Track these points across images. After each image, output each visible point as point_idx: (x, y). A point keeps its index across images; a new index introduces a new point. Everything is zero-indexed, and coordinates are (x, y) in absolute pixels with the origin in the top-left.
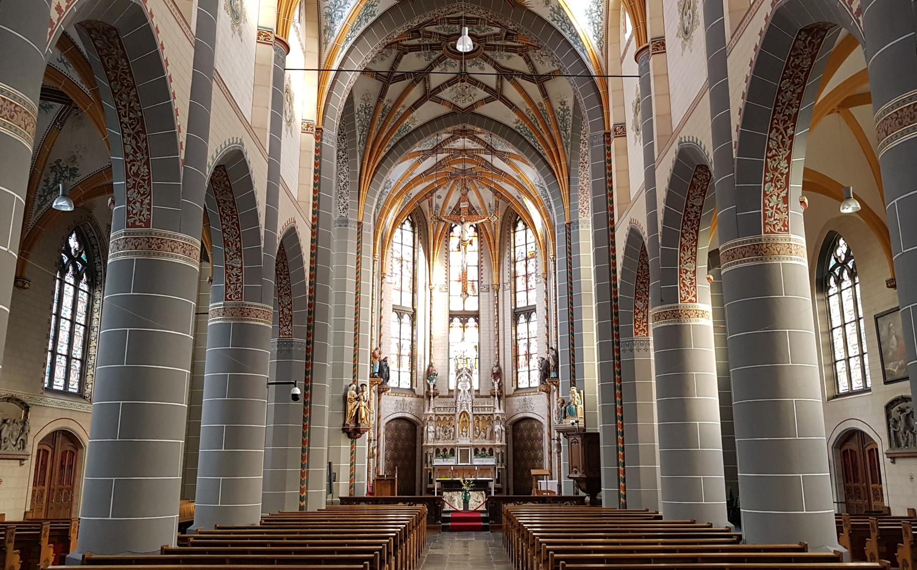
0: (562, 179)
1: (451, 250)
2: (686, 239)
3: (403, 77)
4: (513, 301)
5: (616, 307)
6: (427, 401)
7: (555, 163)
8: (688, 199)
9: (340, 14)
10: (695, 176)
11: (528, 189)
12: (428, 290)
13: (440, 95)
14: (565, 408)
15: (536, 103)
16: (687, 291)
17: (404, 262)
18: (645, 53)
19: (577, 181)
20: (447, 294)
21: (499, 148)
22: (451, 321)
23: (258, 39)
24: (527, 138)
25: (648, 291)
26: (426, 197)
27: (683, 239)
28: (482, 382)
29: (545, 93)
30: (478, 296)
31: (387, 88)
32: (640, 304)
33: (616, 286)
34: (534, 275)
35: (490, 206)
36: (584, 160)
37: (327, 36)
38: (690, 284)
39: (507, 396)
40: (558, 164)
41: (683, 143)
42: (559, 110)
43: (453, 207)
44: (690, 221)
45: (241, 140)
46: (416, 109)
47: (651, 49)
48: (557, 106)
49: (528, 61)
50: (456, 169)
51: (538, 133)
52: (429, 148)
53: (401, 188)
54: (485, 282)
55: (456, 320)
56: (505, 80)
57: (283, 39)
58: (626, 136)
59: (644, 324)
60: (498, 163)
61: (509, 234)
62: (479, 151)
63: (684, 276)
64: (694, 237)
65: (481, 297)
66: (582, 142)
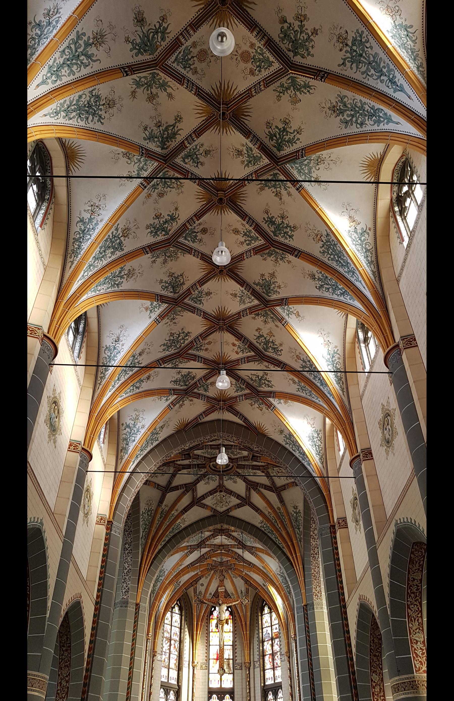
0: (298, 567)
1: (211, 631)
2: (412, 611)
3: (176, 488)
4: (262, 678)
5: (355, 681)
7: (292, 555)
8: (409, 573)
9: (133, 438)
10: (412, 553)
11: (271, 577)
12: (191, 668)
13: (204, 501)
15: (276, 507)
16: (420, 662)
17: (173, 642)
18: (357, 461)
19: (310, 569)
20: (207, 671)
21: (248, 544)
23: (69, 448)
24: (270, 535)
25: (381, 665)
26: (192, 585)
27: (409, 611)
29: (281, 500)
30: (233, 673)
31: (166, 495)
32: (375, 677)
33: (352, 659)
34: (278, 653)
35: (242, 592)
36: (314, 552)
37: (122, 454)
38: (422, 654)
40: (294, 555)
41: (399, 524)
42: (293, 513)
43: (213, 594)
44: (414, 593)
45: (41, 520)
46: (186, 512)
47: (361, 457)
48: (291, 510)
49: (268, 476)
50: (215, 561)
51: (277, 530)
52: (195, 543)
53: (172, 577)
55: (214, 696)
56: (252, 491)
57: (88, 449)
58: (347, 527)
59: (382, 698)
60: (248, 556)
61: (257, 616)
62: (233, 546)
63: (415, 646)
64: (418, 608)
65: (235, 675)
66: (312, 537)
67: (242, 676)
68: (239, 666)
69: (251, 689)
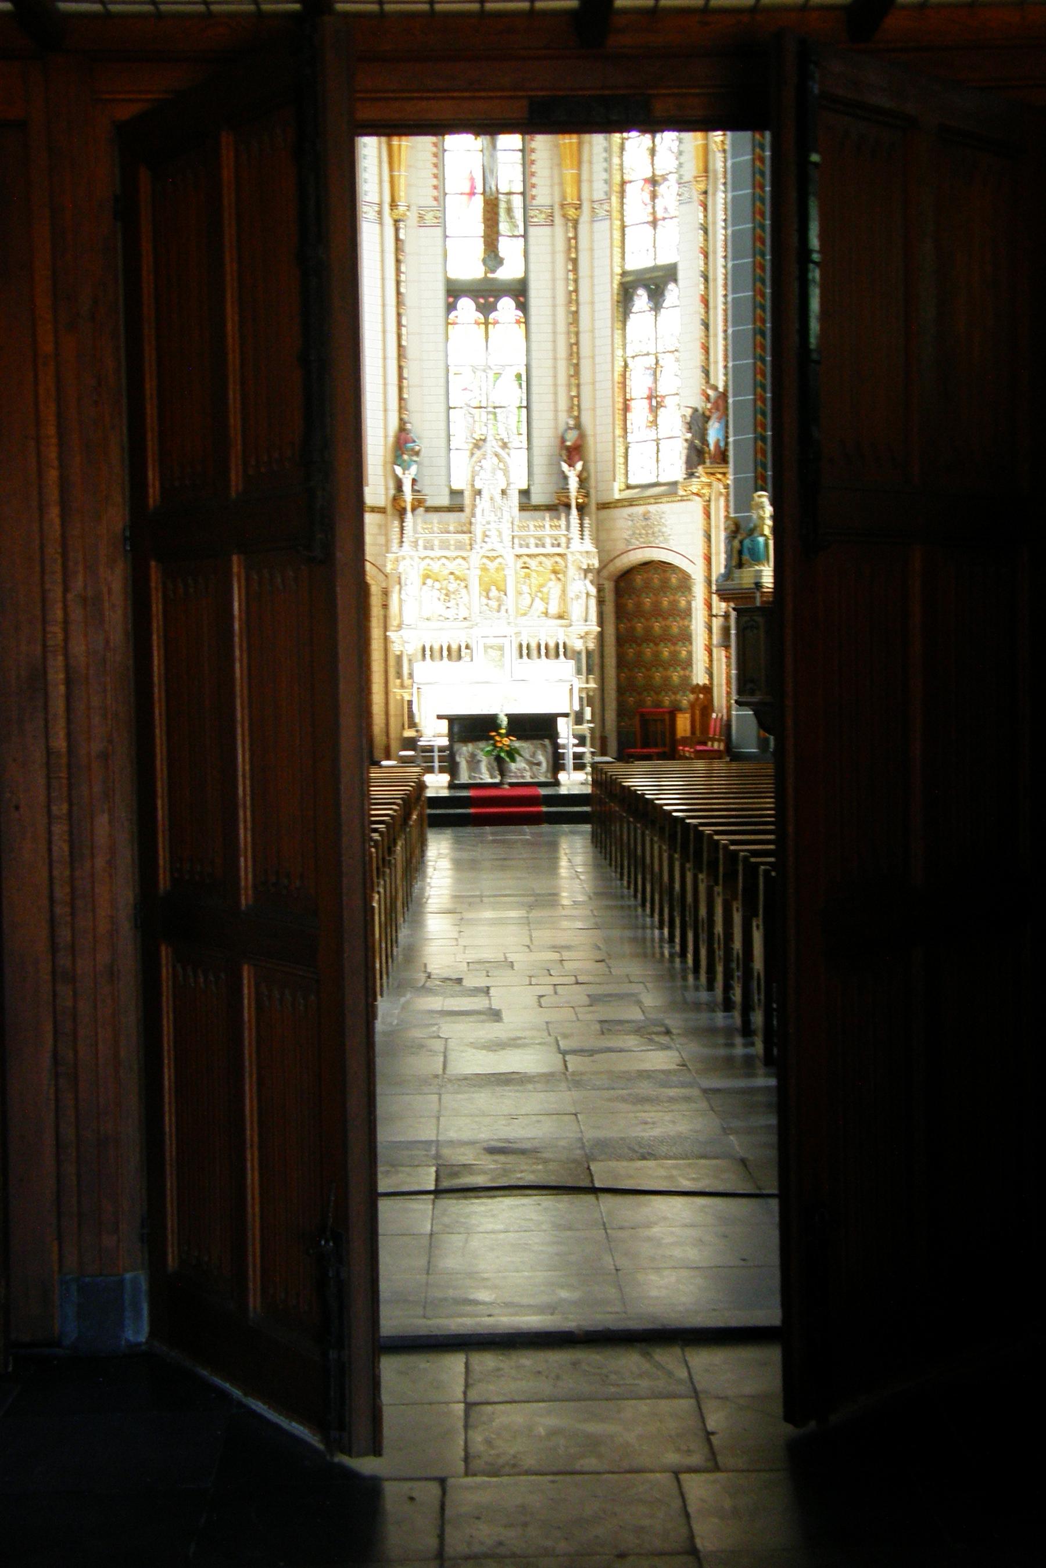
6: (396, 523)
12: (388, 221)
14: (741, 542)
20: (439, 230)
22: (451, 307)
28: (537, 470)
30: (525, 236)
34: (673, 178)
39: (604, 506)
54: (543, 196)
55: (466, 305)
65: (532, 240)
67: (553, 245)
68: (543, 216)
69: (581, 282)
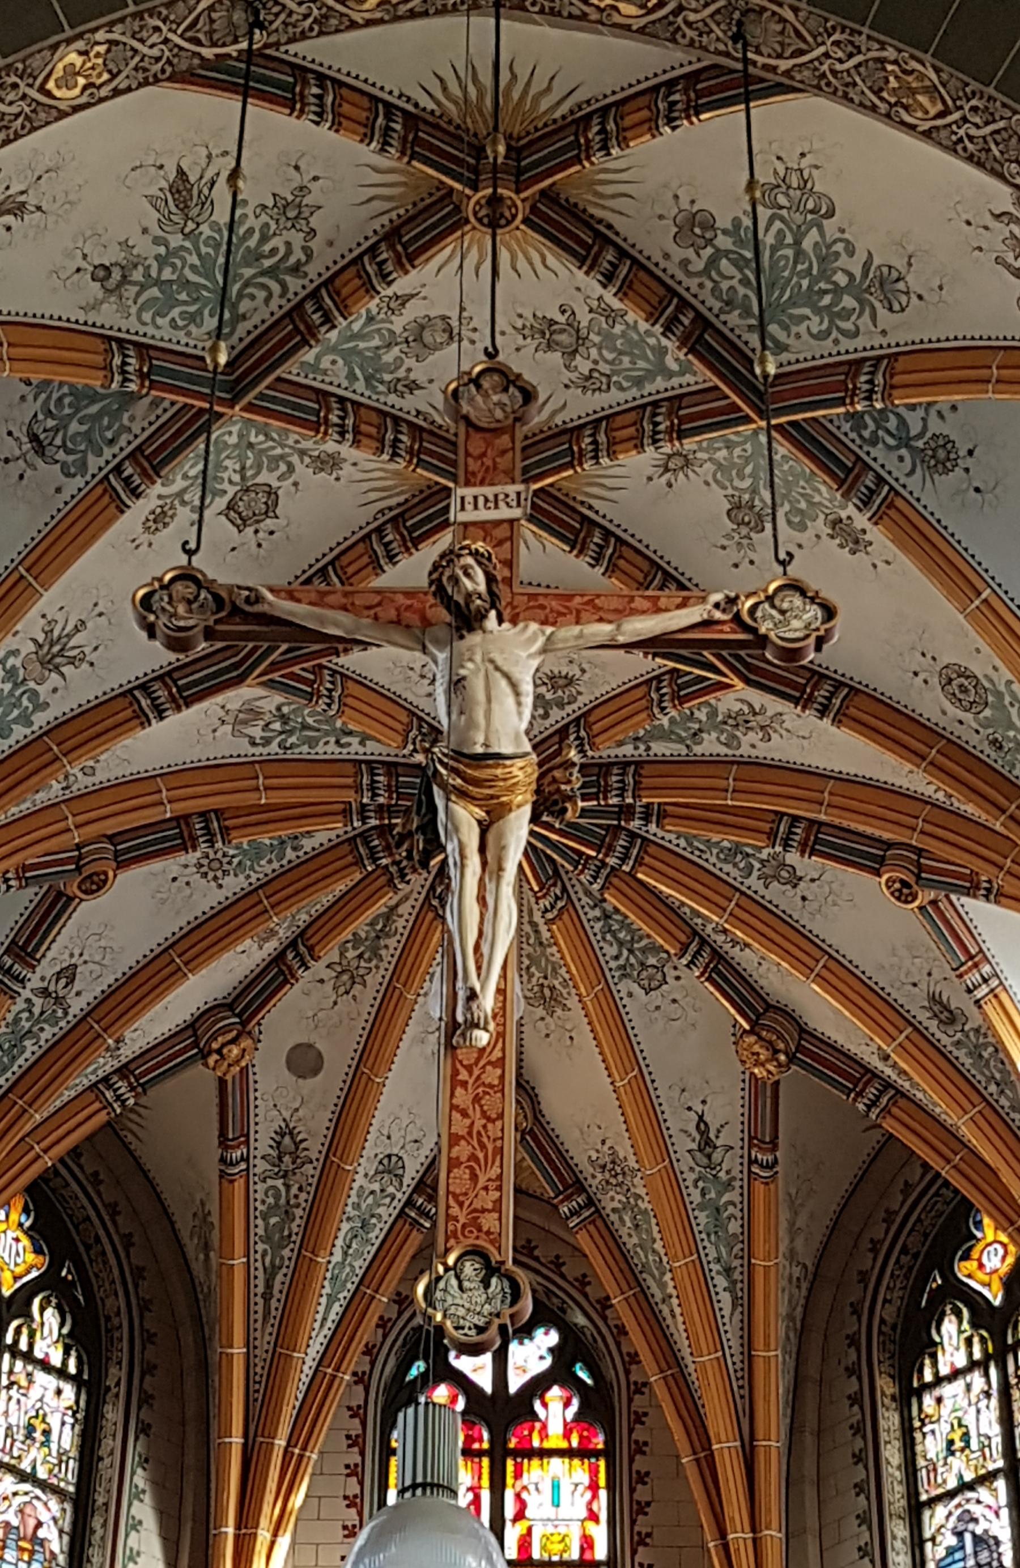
35: (706, 1145)
43: (412, 1172)
